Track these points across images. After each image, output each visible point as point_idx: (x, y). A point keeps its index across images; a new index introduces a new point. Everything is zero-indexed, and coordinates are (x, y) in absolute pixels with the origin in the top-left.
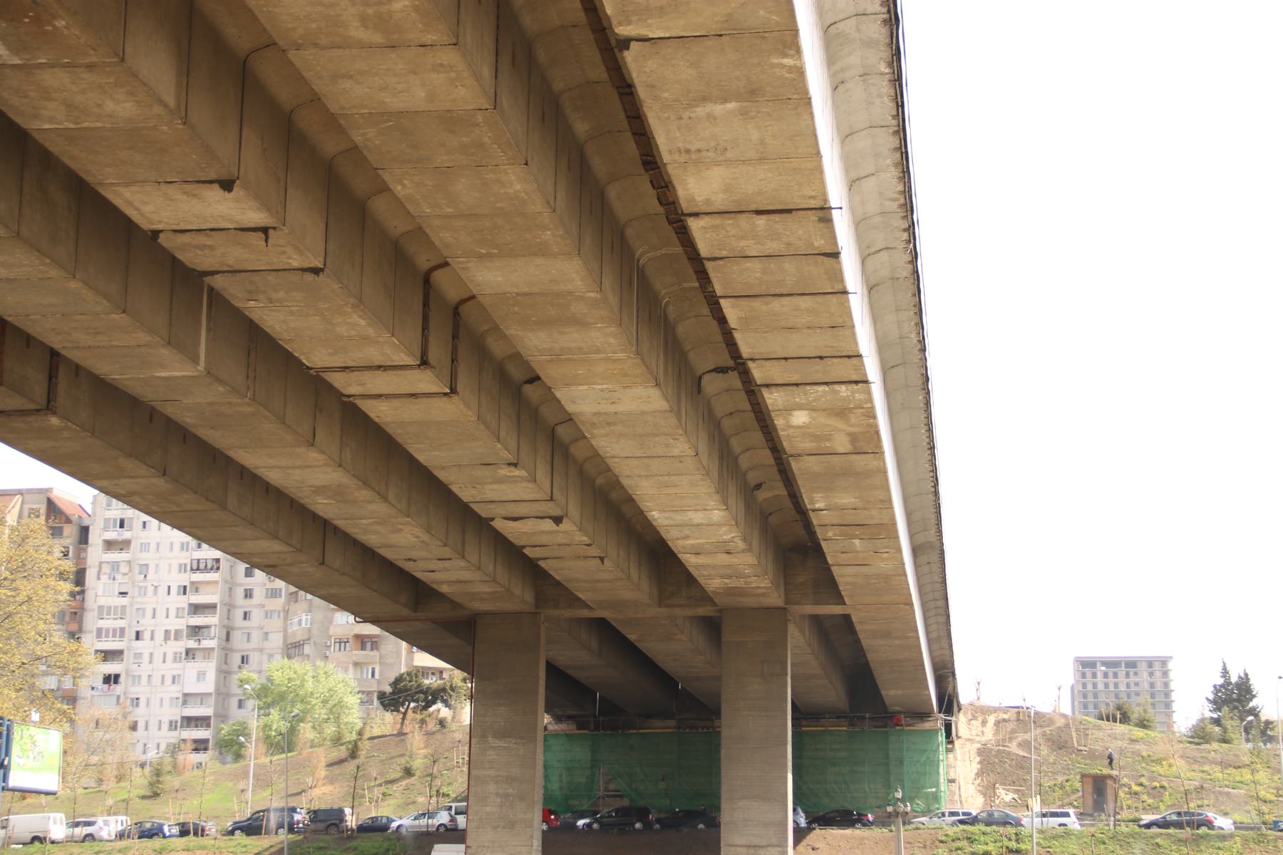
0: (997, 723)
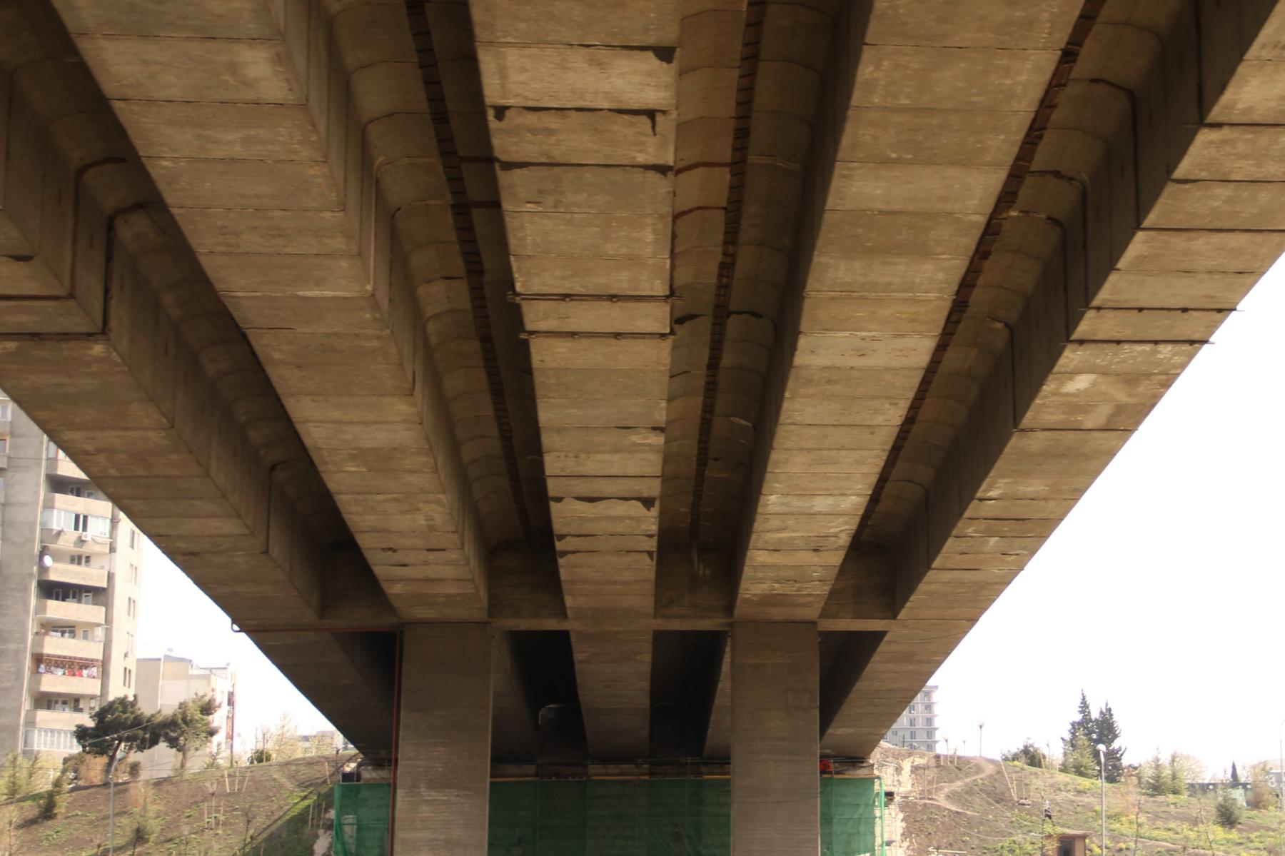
0: (915, 769)
